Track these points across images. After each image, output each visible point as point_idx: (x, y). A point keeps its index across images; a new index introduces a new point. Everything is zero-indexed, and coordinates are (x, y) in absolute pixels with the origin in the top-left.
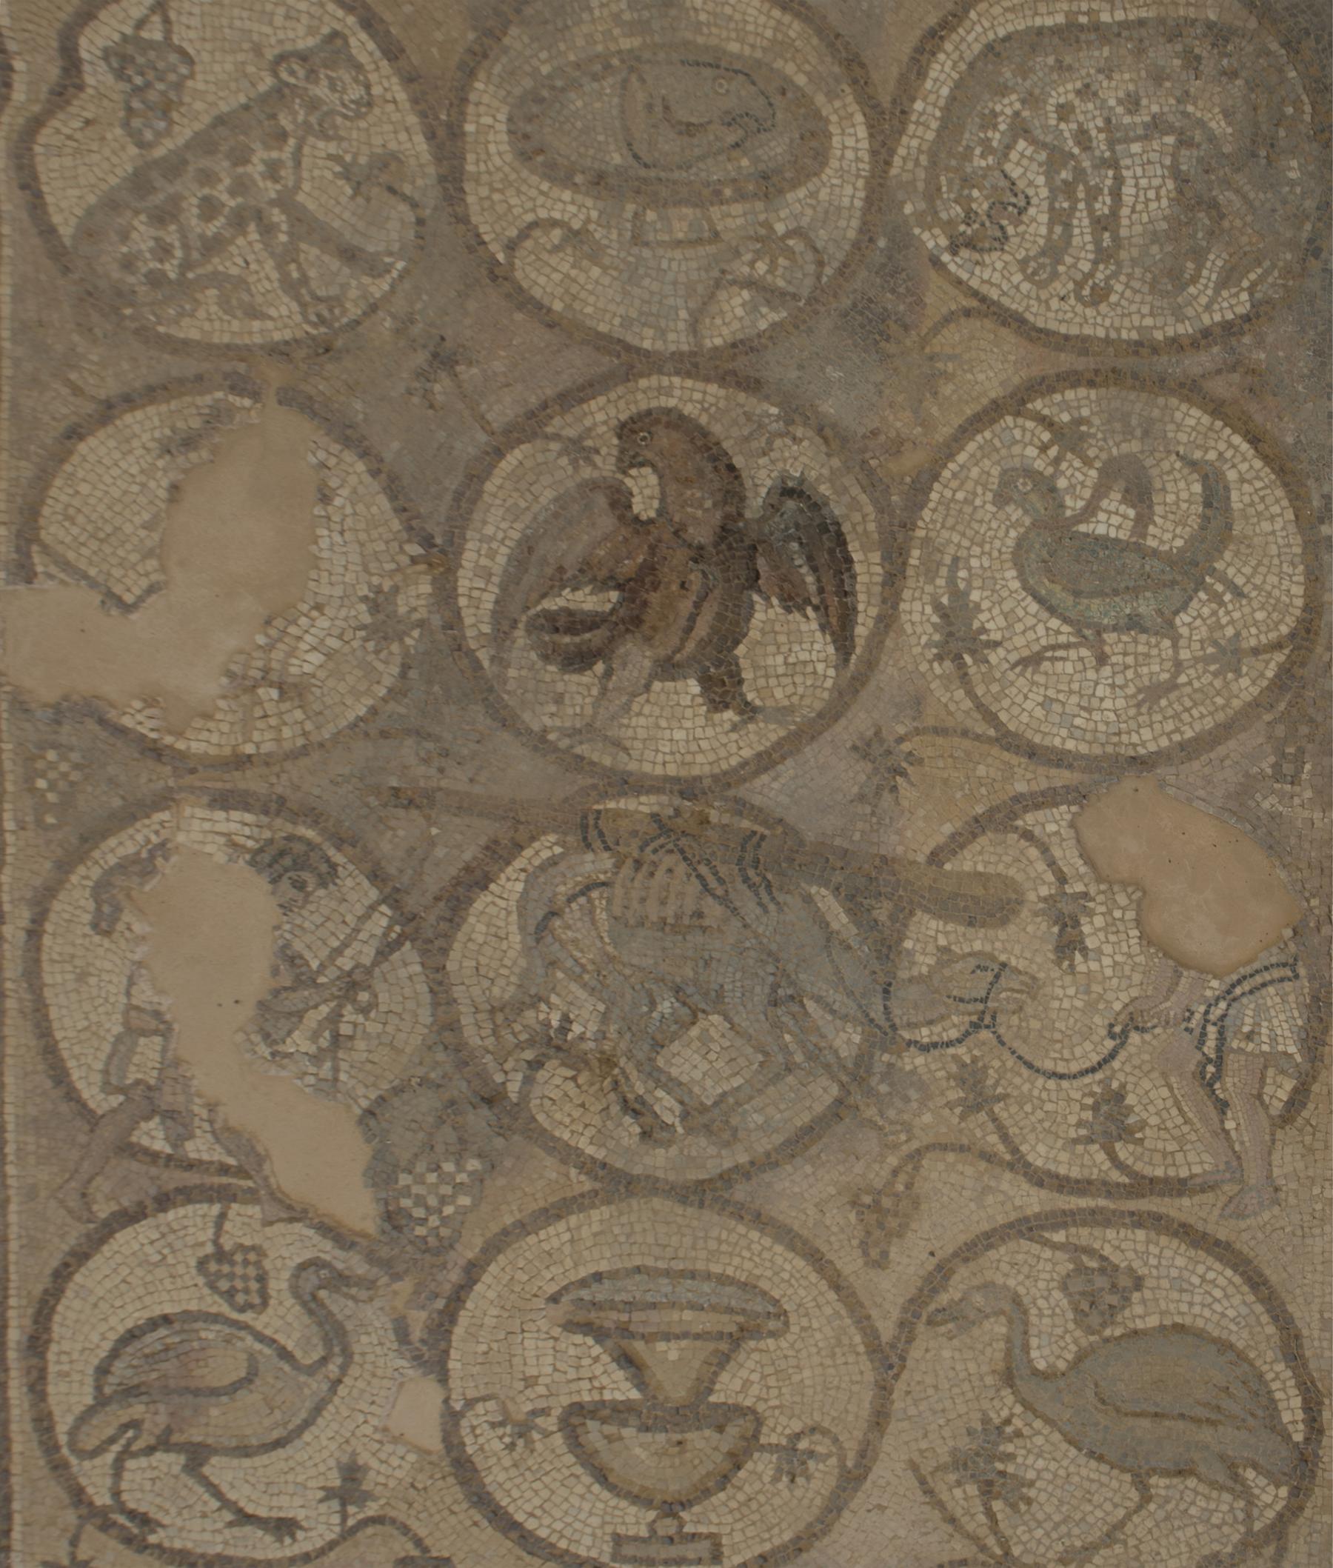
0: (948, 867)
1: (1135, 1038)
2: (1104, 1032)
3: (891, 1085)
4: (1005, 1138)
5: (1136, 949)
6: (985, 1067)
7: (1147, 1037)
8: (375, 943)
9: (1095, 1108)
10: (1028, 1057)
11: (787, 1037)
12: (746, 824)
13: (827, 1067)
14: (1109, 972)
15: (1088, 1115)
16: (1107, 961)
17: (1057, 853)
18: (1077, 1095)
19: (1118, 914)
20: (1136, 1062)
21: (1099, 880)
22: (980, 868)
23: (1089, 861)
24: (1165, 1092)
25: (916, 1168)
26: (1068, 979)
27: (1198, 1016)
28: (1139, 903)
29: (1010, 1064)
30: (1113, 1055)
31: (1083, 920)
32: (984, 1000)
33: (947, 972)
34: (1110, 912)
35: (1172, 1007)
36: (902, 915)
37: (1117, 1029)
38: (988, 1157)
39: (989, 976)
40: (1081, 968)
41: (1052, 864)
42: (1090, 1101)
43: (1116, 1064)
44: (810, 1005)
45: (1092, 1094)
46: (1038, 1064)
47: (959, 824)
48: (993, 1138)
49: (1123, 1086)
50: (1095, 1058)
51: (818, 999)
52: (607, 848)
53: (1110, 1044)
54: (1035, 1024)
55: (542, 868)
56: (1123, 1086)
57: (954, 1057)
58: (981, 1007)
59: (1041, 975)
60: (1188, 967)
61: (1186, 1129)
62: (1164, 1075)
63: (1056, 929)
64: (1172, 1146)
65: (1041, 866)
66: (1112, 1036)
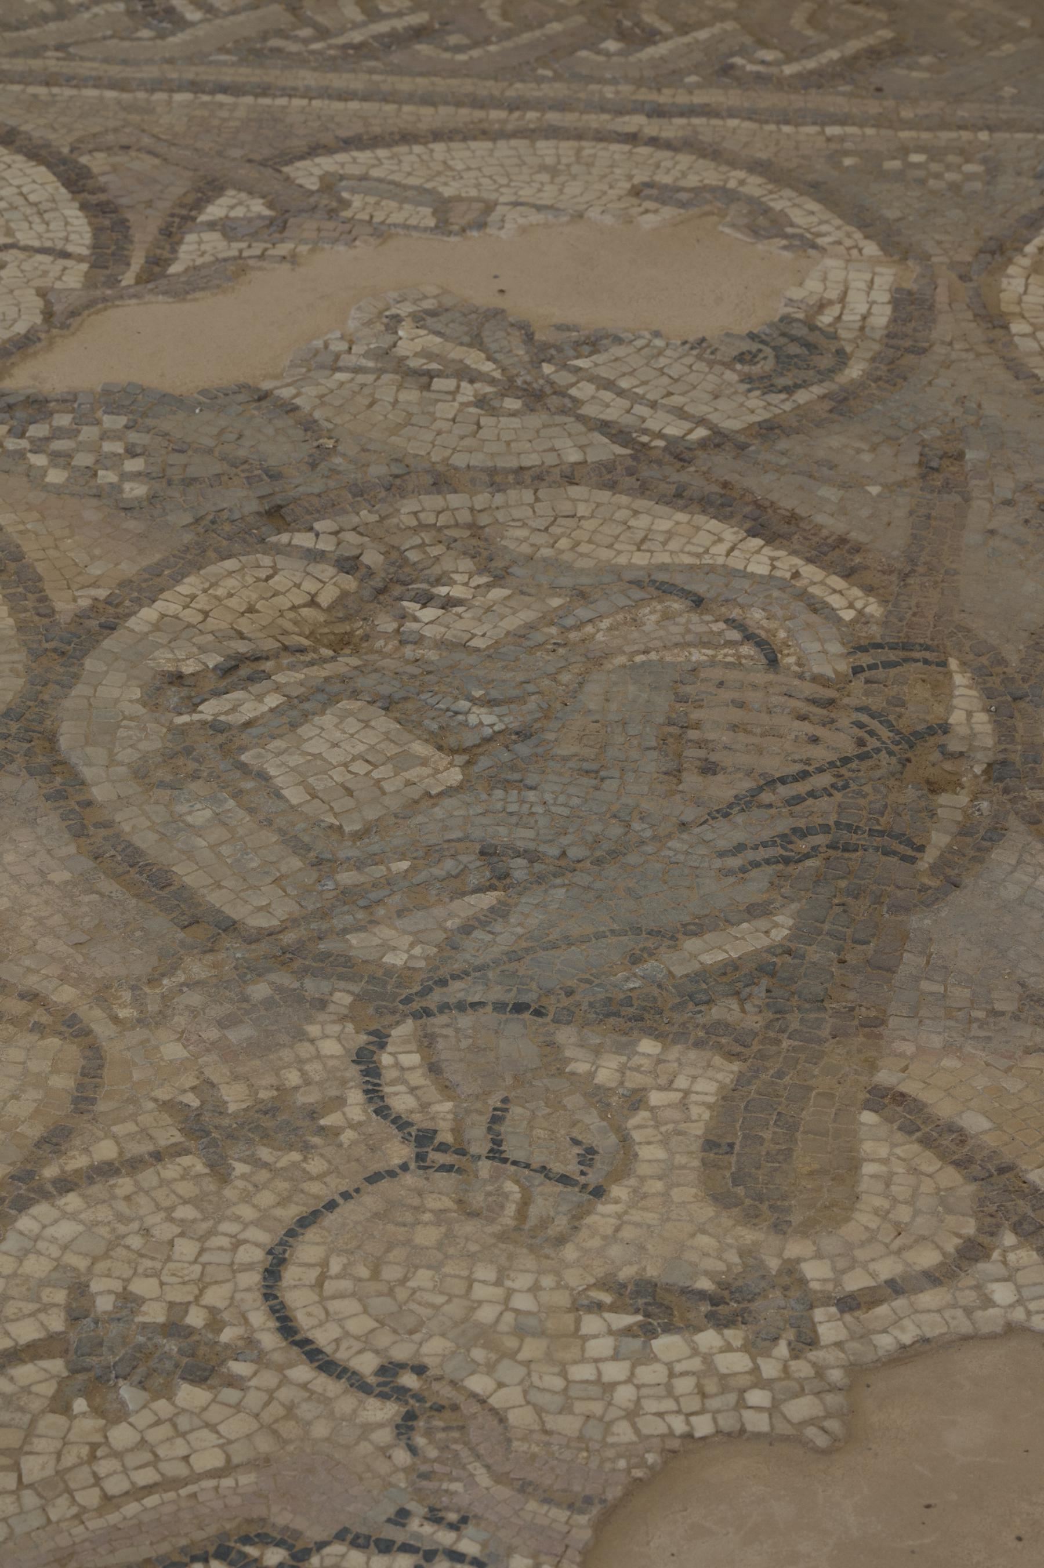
0: (868, 1117)
1: (382, 1412)
2: (401, 1353)
3: (268, 1003)
4: (107, 1170)
5: (651, 1426)
6: (307, 1149)
7: (384, 1436)
8: (627, 420)
9: (174, 1328)
10: (330, 1219)
11: (405, 865)
12: (939, 840)
13: (324, 914)
14: (583, 1372)
15: (155, 1314)
16: (614, 1371)
17: (929, 1298)
18: (215, 1296)
19: (757, 1397)
20: (307, 1410)
21: (855, 1370)
22: (868, 1169)
23: (904, 1355)
24: (209, 1459)
25: (39, 1029)
26: (563, 1299)
27: (446, 1538)
28: (796, 1439)
29: (315, 1188)
30: (328, 1366)
31: (735, 1336)
32: (496, 1154)
33: (574, 1101)
34: (761, 1383)
35: (475, 1484)
36: (729, 1041)
37: (409, 1380)
38: (55, 1140)
39: (572, 1168)
40: (591, 1324)
41: (895, 1288)
42: (196, 1318)
43: (302, 1372)
44: (489, 899)
45: (215, 1323)
46: (312, 1234)
47: (991, 1141)
48: (106, 1151)
49: (234, 1382)
50: (323, 1338)
51: (500, 912)
52: (857, 670)
53: (366, 1364)
54: (427, 1236)
55: (803, 595)
56: (234, 1382)
57: (340, 1102)
58: (479, 1146)
59: (570, 1253)
60: (599, 1526)
61: (90, 1498)
62: (261, 1463)
63: (704, 1284)
64: (34, 1468)
65: (887, 1269)
66: (389, 1370)
